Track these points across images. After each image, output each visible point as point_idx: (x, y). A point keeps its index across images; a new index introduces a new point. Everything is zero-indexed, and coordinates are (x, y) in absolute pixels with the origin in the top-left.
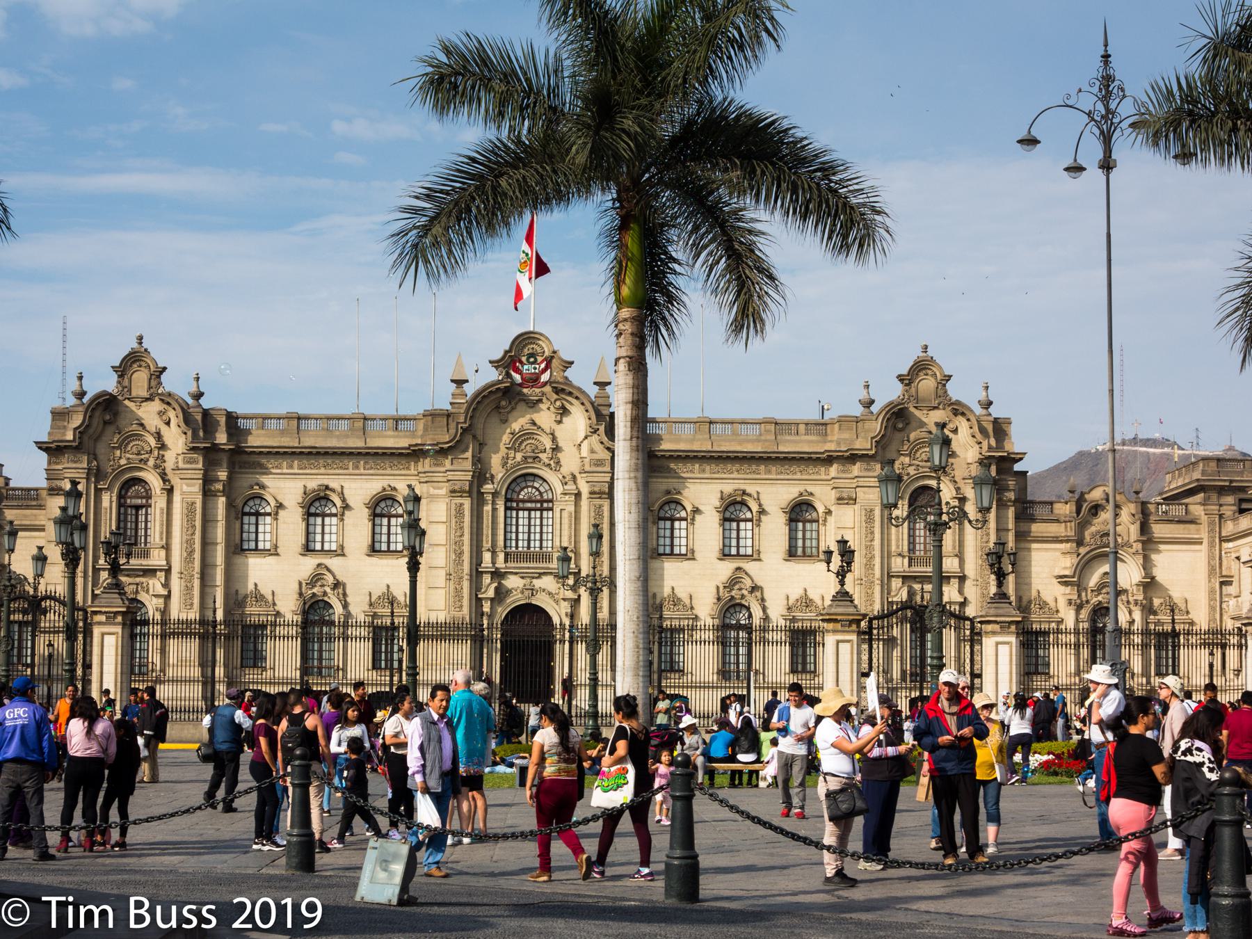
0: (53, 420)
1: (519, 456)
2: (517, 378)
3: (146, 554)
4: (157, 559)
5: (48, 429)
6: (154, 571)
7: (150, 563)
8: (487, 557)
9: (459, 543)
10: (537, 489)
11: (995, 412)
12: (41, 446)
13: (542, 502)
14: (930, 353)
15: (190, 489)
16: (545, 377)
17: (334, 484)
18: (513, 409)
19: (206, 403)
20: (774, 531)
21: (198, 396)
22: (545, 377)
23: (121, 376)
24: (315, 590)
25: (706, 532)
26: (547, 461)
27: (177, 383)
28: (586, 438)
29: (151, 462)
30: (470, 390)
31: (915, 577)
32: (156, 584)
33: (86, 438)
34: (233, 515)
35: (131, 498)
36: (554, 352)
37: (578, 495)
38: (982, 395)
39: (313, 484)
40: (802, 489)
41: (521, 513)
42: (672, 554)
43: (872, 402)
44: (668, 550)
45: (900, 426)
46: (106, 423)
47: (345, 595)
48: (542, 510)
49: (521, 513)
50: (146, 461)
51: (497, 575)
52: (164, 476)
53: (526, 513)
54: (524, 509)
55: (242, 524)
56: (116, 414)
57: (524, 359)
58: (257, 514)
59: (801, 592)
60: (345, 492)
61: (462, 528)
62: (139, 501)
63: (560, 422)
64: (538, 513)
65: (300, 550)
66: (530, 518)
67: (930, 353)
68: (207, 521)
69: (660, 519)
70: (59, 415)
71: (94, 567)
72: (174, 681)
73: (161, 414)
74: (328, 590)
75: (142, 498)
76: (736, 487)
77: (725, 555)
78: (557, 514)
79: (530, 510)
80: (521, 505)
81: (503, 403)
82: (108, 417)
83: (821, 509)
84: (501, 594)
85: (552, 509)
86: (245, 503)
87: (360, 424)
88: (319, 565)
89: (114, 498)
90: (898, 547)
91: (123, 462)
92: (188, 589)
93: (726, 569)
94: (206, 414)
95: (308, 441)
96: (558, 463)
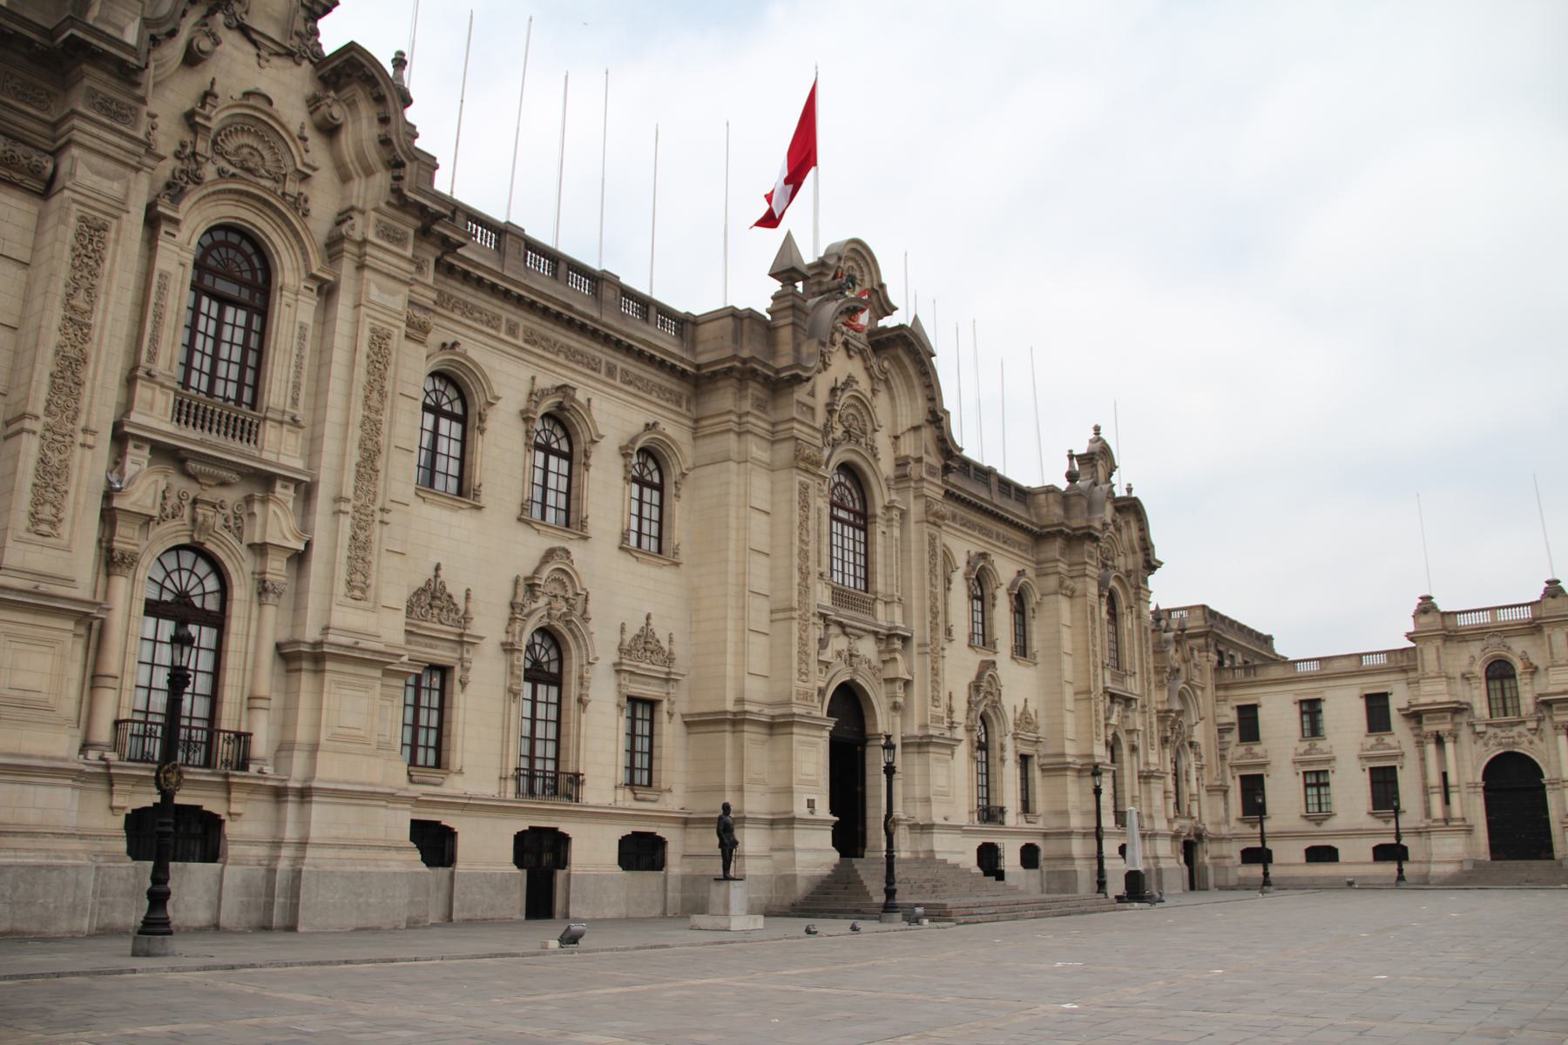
1: (839, 432)
3: (247, 431)
4: (279, 448)
7: (265, 455)
15: (387, 300)
28: (916, 429)
32: (277, 522)
35: (215, 273)
36: (882, 286)
37: (903, 514)
39: (546, 381)
62: (231, 289)
71: (117, 426)
75: (241, 283)
78: (879, 539)
82: (205, 44)
83: (1033, 599)
89: (189, 259)
92: (360, 547)
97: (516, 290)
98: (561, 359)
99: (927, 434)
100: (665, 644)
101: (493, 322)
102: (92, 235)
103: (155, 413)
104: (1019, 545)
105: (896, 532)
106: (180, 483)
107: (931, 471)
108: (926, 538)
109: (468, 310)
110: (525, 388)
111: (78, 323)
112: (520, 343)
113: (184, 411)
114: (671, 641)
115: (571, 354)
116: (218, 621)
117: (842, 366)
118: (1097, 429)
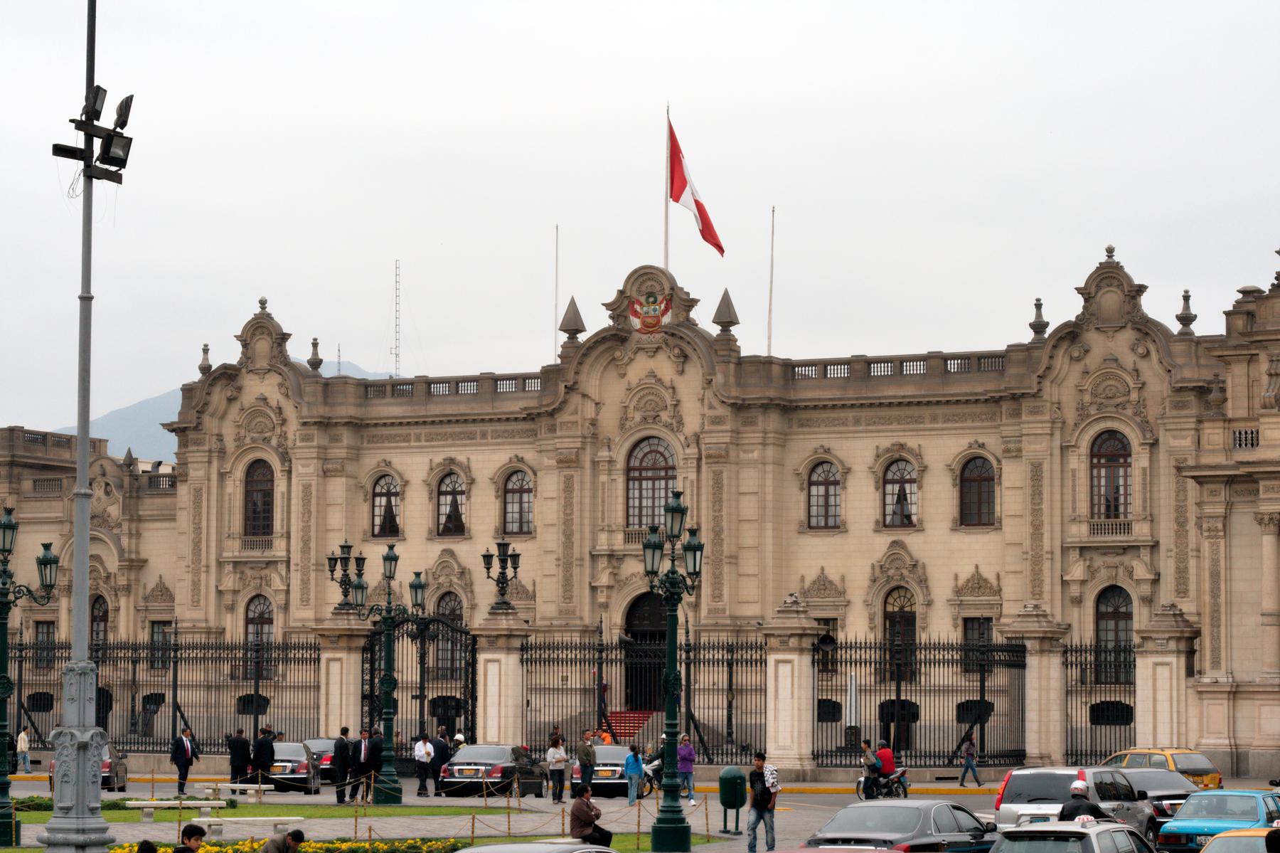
0: (184, 397)
1: (638, 416)
2: (636, 323)
3: (269, 545)
5: (179, 408)
6: (276, 562)
8: (603, 538)
9: (568, 523)
10: (662, 454)
11: (1198, 329)
12: (171, 428)
13: (667, 469)
14: (1116, 258)
16: (666, 319)
17: (461, 457)
18: (632, 360)
19: (326, 372)
20: (937, 498)
21: (316, 363)
22: (666, 319)
23: (245, 345)
24: (441, 580)
25: (861, 500)
26: (669, 420)
27: (298, 352)
29: (274, 442)
30: (582, 337)
31: (1097, 548)
33: (206, 418)
34: (361, 497)
37: (699, 459)
38: (1179, 310)
39: (439, 458)
40: (972, 440)
41: (644, 483)
42: (826, 527)
43: (1047, 324)
44: (823, 524)
45: (1076, 354)
46: (231, 400)
47: (472, 584)
48: (667, 478)
49: (644, 483)
50: (267, 440)
51: (614, 558)
52: (285, 458)
53: (650, 483)
54: (648, 479)
55: (374, 506)
56: (239, 389)
57: (643, 299)
58: (389, 495)
59: (972, 569)
60: (473, 466)
61: (571, 505)
63: (682, 372)
64: (663, 482)
65: (425, 534)
66: (653, 489)
67: (1116, 258)
68: (324, 504)
69: (811, 484)
70: (188, 390)
72: (294, 687)
73: (281, 385)
74: (455, 580)
76: (895, 440)
77: (883, 525)
79: (653, 479)
80: (644, 474)
81: (617, 354)
82: (229, 394)
84: (617, 583)
85: (674, 478)
86: (376, 483)
87: (487, 385)
88: (444, 550)
89: (238, 483)
90: (1074, 510)
91: (248, 440)
92: (305, 583)
93: (882, 542)
94: (327, 385)
95: (435, 409)
96: (680, 422)
97: (405, 421)
98: (450, 442)
99: (709, 394)
100: (530, 588)
101: (406, 439)
102: (198, 492)
103: (233, 549)
104: (974, 417)
105: (693, 476)
106: (249, 572)
107: (717, 421)
108: (711, 475)
109: (390, 438)
110: (427, 467)
111: (198, 529)
112: (424, 443)
113: (246, 545)
114: (534, 584)
115: (453, 436)
116: (270, 621)
117: (639, 368)
118: (1110, 251)
